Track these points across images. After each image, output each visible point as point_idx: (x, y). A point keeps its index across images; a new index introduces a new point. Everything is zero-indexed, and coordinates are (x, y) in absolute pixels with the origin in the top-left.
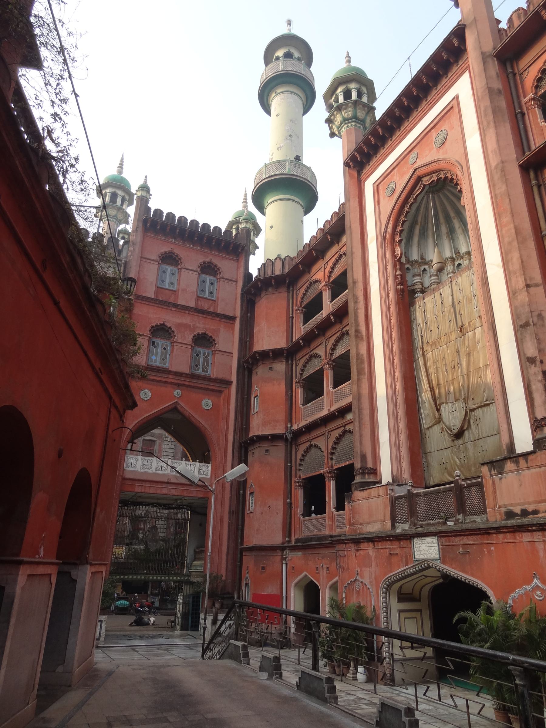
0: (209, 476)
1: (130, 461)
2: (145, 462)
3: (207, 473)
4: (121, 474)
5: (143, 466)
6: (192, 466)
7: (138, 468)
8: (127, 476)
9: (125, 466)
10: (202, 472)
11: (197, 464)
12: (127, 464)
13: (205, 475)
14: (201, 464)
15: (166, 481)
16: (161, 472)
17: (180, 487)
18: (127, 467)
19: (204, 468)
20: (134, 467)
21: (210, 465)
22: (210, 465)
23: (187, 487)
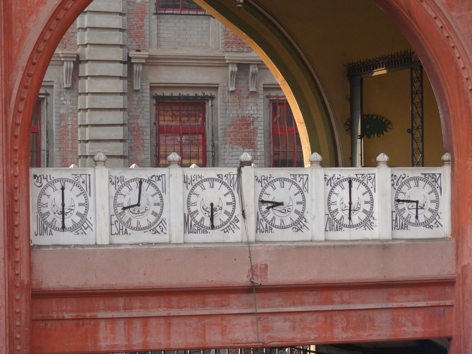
0: (445, 228)
1: (54, 196)
2: (130, 197)
3: (435, 212)
4: (24, 276)
5: (123, 213)
6: (358, 191)
7: (100, 232)
8: (54, 277)
9: (34, 227)
10: (409, 211)
11: (382, 174)
12: (42, 216)
13: (427, 224)
14: (399, 172)
15: (243, 279)
16: (215, 236)
17: (310, 304)
18: (43, 230)
19: (420, 193)
20: (76, 228)
21: (445, 173)
22: (445, 173)
23: (346, 295)
